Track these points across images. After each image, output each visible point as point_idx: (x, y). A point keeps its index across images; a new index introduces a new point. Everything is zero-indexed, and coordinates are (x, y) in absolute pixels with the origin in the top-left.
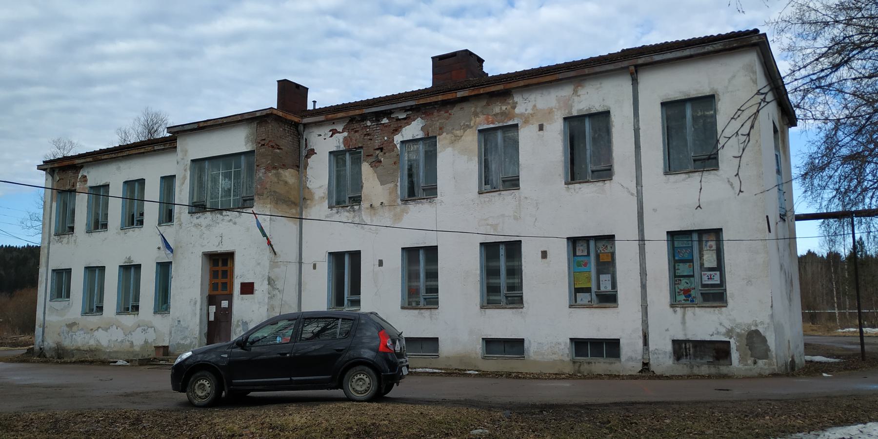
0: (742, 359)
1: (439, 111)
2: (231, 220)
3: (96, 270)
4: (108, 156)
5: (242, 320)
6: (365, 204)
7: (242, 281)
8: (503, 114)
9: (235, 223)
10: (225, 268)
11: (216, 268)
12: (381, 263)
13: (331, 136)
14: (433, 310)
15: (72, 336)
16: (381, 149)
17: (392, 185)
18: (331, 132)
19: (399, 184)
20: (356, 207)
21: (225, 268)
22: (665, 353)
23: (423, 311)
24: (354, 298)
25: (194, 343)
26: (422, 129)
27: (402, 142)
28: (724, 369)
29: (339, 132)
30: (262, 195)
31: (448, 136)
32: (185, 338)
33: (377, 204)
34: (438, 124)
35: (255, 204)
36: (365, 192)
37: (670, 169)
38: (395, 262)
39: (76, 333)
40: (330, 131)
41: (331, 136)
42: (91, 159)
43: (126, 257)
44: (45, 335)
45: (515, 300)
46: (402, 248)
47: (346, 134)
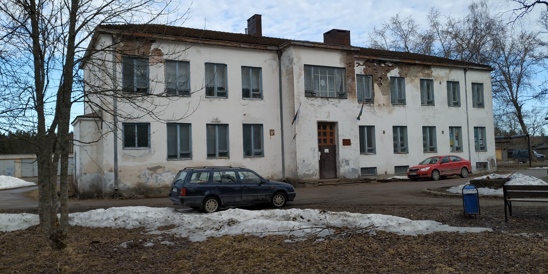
0: (490, 168)
1: (405, 67)
3: (135, 125)
4: (193, 40)
6: (376, 104)
7: (344, 138)
8: (428, 74)
9: (337, 106)
10: (325, 131)
11: (320, 131)
12: (384, 132)
13: (357, 66)
14: (406, 154)
15: (157, 177)
16: (381, 78)
17: (388, 96)
18: (357, 64)
19: (390, 96)
20: (372, 105)
21: (325, 131)
22: (475, 167)
23: (402, 154)
25: (315, 173)
27: (390, 77)
28: (487, 171)
29: (361, 65)
30: (352, 93)
31: (409, 78)
35: (348, 97)
37: (474, 106)
38: (390, 132)
39: (162, 175)
40: (357, 63)
41: (357, 66)
42: (174, 39)
43: (213, 118)
44: (119, 178)
47: (364, 67)
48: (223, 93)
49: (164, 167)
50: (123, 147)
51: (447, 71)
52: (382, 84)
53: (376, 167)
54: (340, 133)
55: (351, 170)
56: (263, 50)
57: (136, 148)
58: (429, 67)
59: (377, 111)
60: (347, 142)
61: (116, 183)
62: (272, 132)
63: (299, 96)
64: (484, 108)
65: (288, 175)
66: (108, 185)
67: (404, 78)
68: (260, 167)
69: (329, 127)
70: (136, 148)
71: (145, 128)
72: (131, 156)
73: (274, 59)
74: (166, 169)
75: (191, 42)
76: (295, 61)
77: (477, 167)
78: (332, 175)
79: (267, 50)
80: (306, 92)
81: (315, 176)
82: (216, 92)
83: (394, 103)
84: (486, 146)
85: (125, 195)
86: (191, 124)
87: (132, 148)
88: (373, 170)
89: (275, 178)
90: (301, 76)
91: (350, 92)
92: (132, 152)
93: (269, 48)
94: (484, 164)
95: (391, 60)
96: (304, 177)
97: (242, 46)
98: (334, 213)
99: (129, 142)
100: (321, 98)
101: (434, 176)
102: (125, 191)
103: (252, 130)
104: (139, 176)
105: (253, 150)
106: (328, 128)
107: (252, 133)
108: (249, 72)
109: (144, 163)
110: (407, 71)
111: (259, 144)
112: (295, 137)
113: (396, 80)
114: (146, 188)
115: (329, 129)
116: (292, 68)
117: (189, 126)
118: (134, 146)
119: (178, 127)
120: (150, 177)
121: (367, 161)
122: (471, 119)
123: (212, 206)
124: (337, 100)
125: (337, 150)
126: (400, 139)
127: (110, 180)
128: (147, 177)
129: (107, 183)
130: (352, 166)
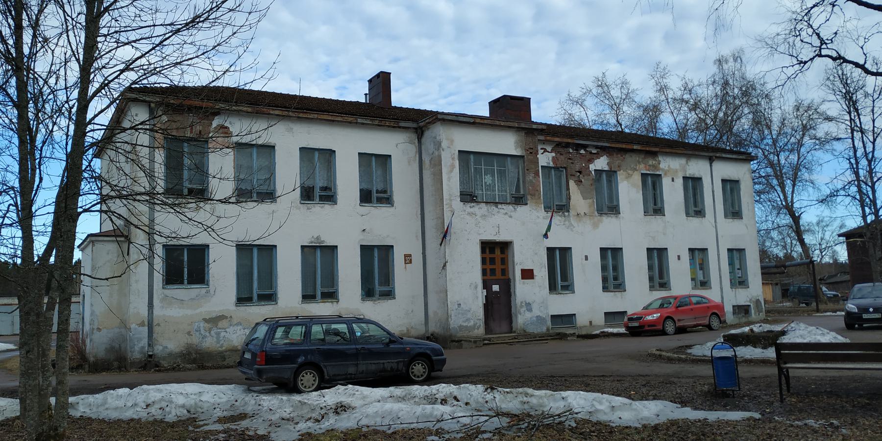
0: (755, 313)
1: (617, 154)
2: (506, 213)
4: (281, 112)
5: (525, 301)
6: (572, 212)
7: (522, 268)
8: (653, 166)
9: (511, 217)
10: (492, 256)
12: (586, 258)
13: (542, 154)
15: (218, 334)
16: (580, 172)
17: (591, 201)
19: (595, 200)
20: (566, 214)
21: (492, 256)
23: (616, 293)
24: (565, 284)
26: (608, 164)
28: (750, 319)
29: (548, 152)
30: (534, 195)
31: (625, 173)
32: (468, 320)
33: (582, 214)
34: (617, 163)
35: (528, 202)
36: (572, 202)
37: (726, 216)
38: (596, 257)
39: (228, 330)
40: (542, 149)
41: (542, 154)
42: (250, 110)
44: (155, 335)
45: (568, 287)
46: (601, 248)
47: (553, 154)
48: (328, 196)
49: (231, 317)
50: (163, 285)
51: (683, 161)
52: (582, 182)
53: (575, 315)
54: (517, 259)
55: (535, 319)
56: (394, 127)
57: (184, 287)
58: (654, 154)
59: (575, 224)
60: (528, 274)
61: (149, 345)
62: (408, 259)
63: (451, 200)
64: (742, 218)
65: (433, 328)
66: (137, 348)
67: (615, 172)
68: (388, 316)
69: (499, 251)
70: (184, 287)
71: (199, 253)
72: (176, 299)
73: (411, 142)
74: (235, 321)
75: (277, 115)
76: (444, 144)
77: (734, 313)
78: (505, 327)
79: (400, 127)
80: (462, 194)
81: (478, 329)
82: (318, 194)
83: (601, 211)
84: (747, 280)
85: (165, 364)
86: (275, 246)
87: (178, 287)
88: (570, 318)
89: (413, 333)
90: (453, 169)
91: (531, 195)
92: (179, 292)
93: (402, 124)
94: (745, 307)
95: (595, 143)
96: (460, 331)
97: (359, 120)
98: (508, 390)
99: (173, 277)
100: (487, 203)
101: (667, 328)
102: (164, 359)
103: (376, 254)
104: (189, 333)
105: (378, 288)
106: (498, 252)
107: (376, 259)
108: (371, 161)
109: (198, 311)
110: (620, 161)
111: (387, 278)
112: (445, 265)
113: (604, 176)
114: (201, 352)
115: (499, 253)
116: (440, 156)
117: (272, 249)
118: (182, 283)
119: (255, 251)
120: (208, 334)
121: (561, 304)
122: (722, 237)
123: (308, 381)
124: (511, 207)
125: (512, 287)
126: (611, 268)
127: (139, 340)
128: (202, 335)
129: (135, 345)
130: (536, 312)
